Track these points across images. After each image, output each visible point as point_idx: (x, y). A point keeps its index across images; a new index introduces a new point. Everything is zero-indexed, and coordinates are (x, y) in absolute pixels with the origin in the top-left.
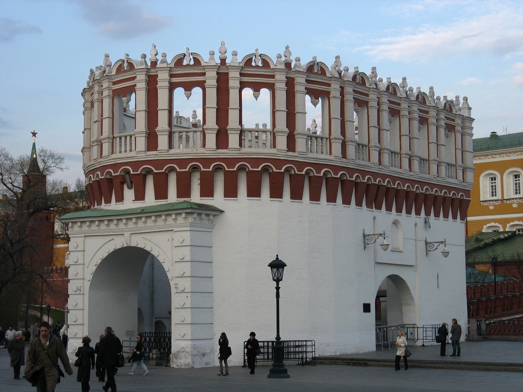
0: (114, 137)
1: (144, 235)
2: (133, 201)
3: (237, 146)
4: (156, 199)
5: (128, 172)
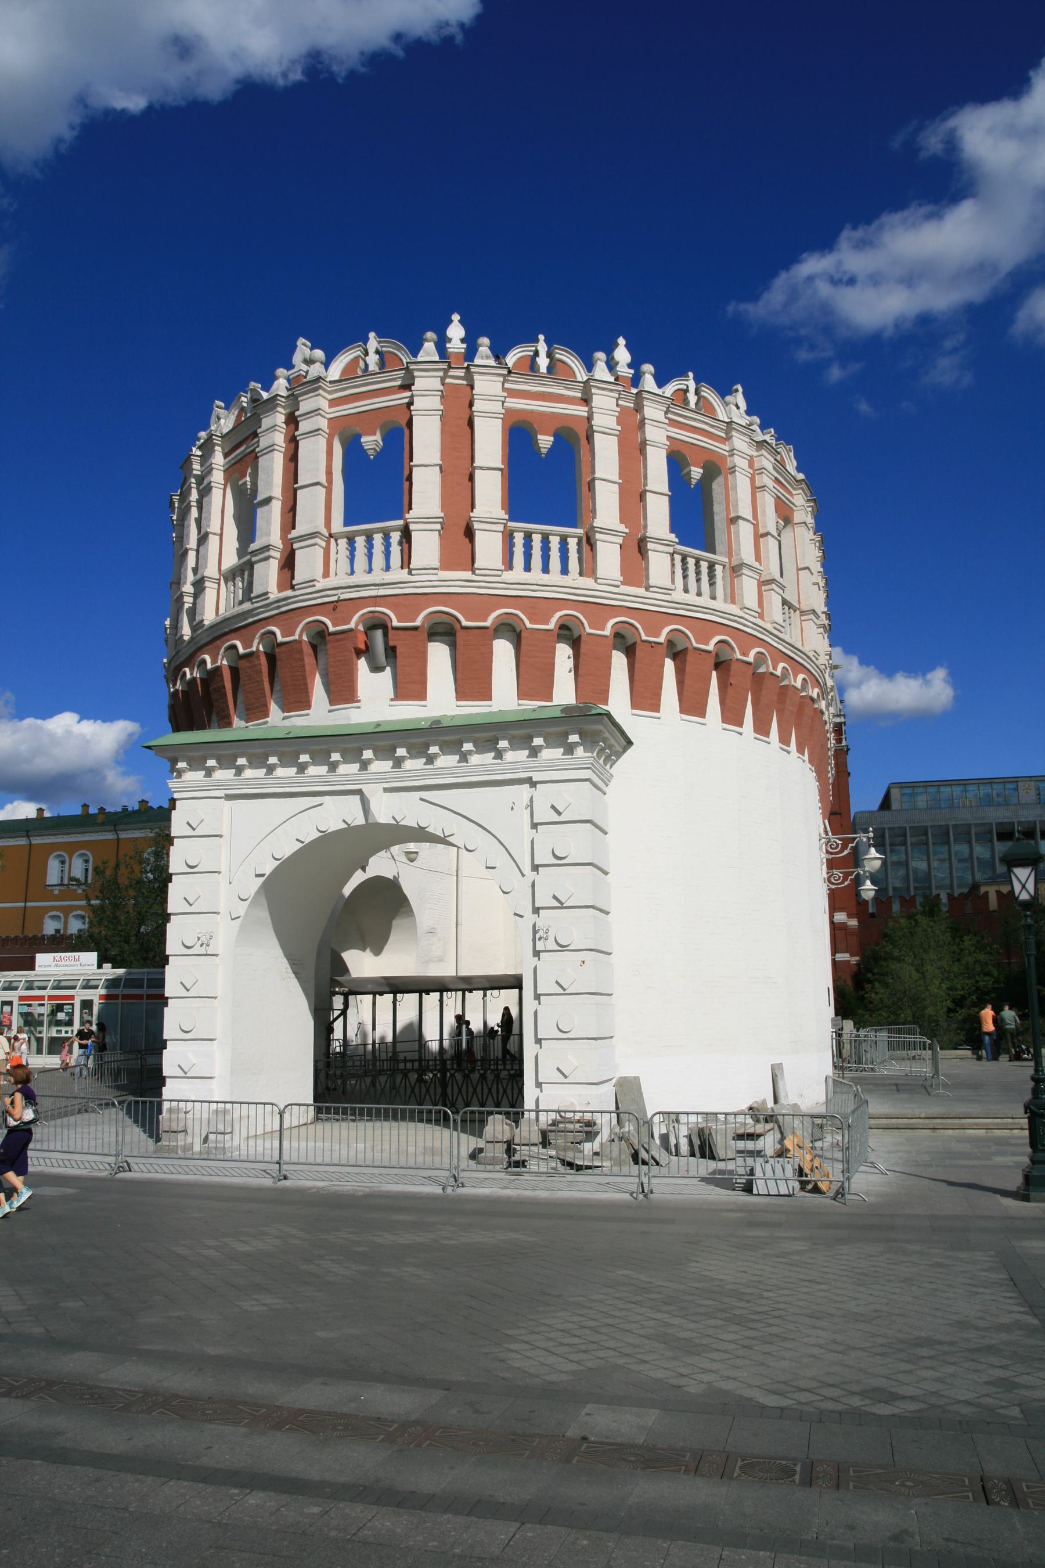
0: (331, 536)
1: (425, 795)
2: (392, 700)
3: (668, 584)
4: (458, 698)
5: (378, 624)
